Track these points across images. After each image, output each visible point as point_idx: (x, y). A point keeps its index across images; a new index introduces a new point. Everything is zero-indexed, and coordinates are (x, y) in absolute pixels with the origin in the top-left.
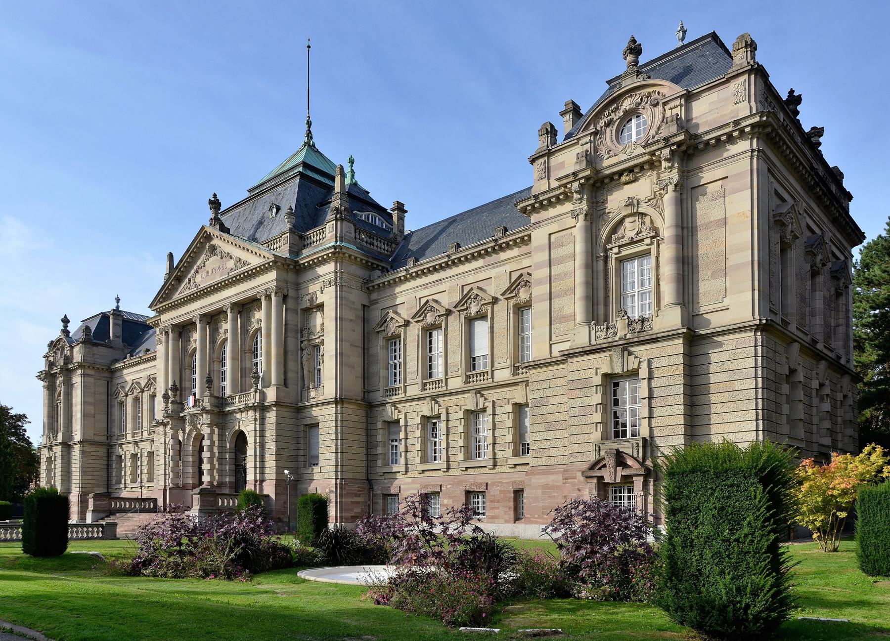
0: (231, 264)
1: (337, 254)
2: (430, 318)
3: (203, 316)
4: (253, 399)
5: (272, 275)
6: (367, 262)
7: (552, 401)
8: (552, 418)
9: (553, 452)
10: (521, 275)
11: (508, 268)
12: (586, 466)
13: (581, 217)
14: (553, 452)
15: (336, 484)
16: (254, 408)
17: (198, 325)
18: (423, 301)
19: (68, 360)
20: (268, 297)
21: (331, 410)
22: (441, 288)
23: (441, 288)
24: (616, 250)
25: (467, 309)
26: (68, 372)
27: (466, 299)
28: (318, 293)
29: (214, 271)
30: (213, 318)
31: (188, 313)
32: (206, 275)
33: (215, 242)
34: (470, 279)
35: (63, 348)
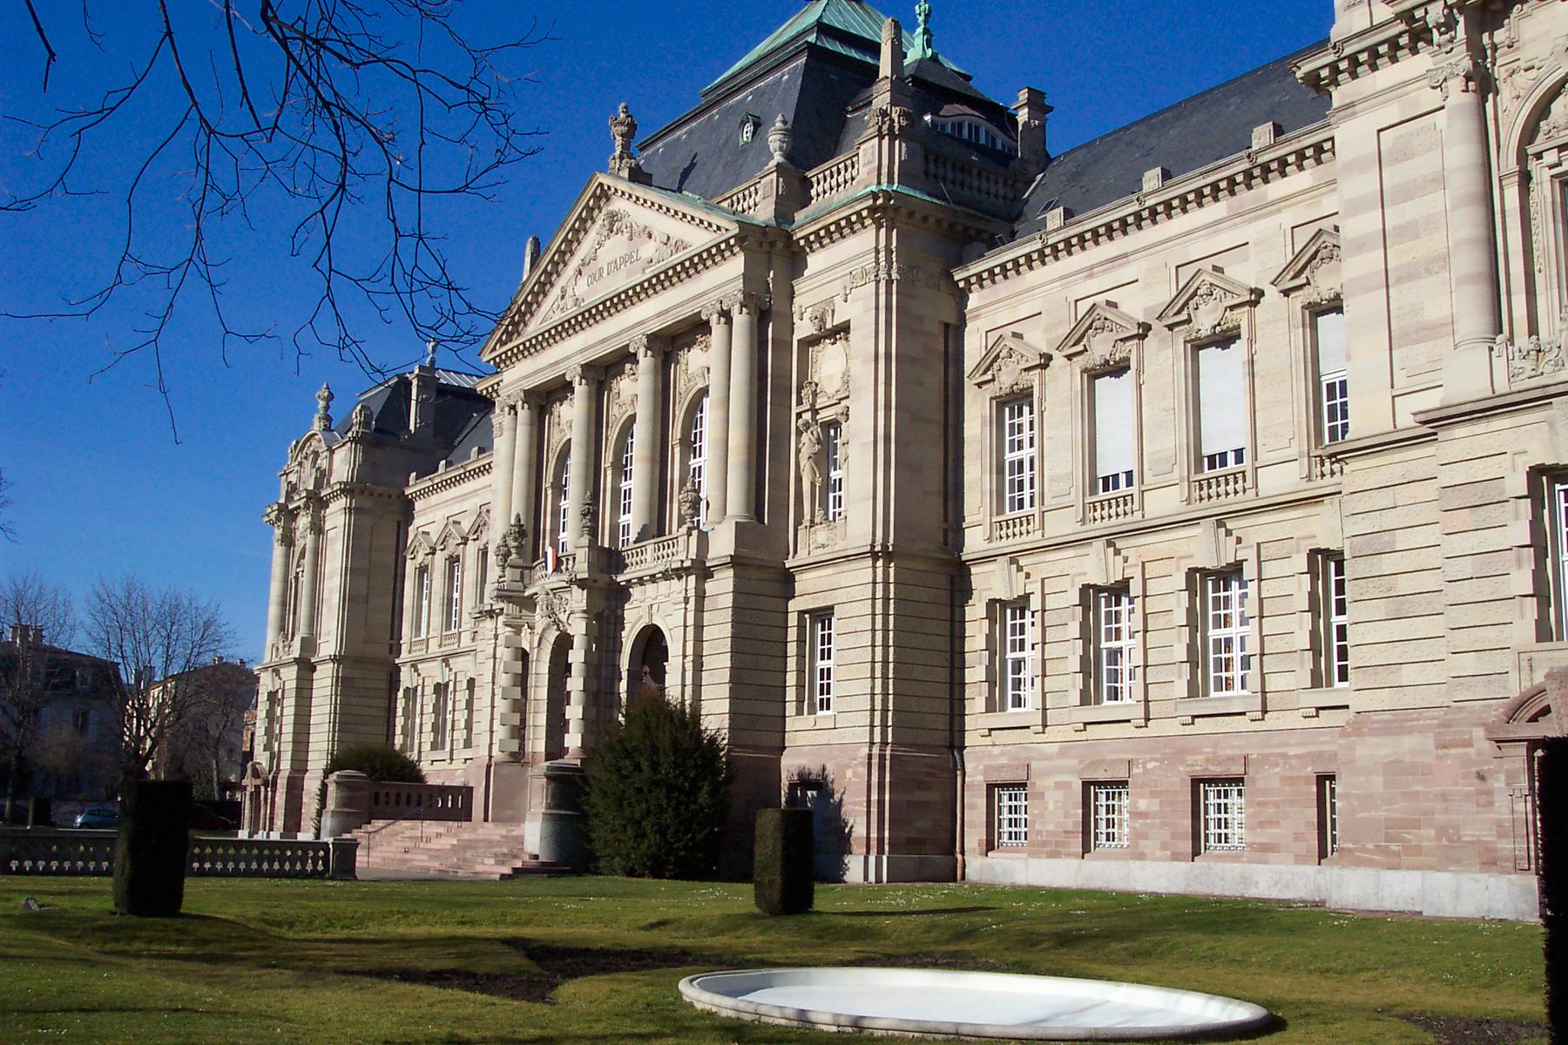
0: (648, 249)
1: (884, 211)
2: (1100, 348)
3: (588, 369)
4: (684, 551)
5: (735, 265)
6: (952, 226)
7: (1402, 540)
8: (1405, 584)
9: (1408, 675)
10: (1320, 232)
11: (1288, 218)
12: (1496, 712)
13: (1456, 84)
14: (1408, 675)
15: (870, 756)
16: (679, 573)
17: (577, 388)
18: (1084, 307)
19: (322, 477)
20: (726, 315)
21: (862, 573)
22: (1126, 274)
23: (1126, 274)
24: (1550, 157)
25: (1189, 321)
26: (317, 502)
27: (1185, 300)
28: (838, 300)
29: (615, 266)
30: (604, 372)
31: (557, 363)
32: (596, 277)
33: (618, 204)
34: (1197, 249)
35: (316, 454)
